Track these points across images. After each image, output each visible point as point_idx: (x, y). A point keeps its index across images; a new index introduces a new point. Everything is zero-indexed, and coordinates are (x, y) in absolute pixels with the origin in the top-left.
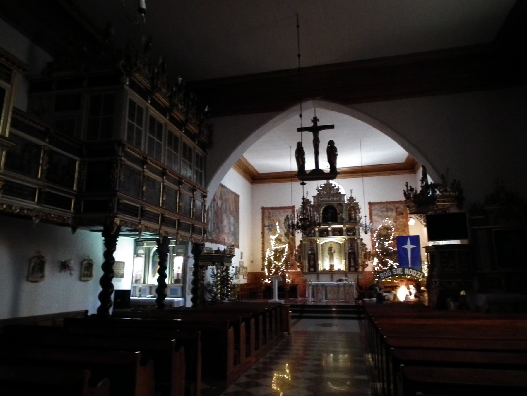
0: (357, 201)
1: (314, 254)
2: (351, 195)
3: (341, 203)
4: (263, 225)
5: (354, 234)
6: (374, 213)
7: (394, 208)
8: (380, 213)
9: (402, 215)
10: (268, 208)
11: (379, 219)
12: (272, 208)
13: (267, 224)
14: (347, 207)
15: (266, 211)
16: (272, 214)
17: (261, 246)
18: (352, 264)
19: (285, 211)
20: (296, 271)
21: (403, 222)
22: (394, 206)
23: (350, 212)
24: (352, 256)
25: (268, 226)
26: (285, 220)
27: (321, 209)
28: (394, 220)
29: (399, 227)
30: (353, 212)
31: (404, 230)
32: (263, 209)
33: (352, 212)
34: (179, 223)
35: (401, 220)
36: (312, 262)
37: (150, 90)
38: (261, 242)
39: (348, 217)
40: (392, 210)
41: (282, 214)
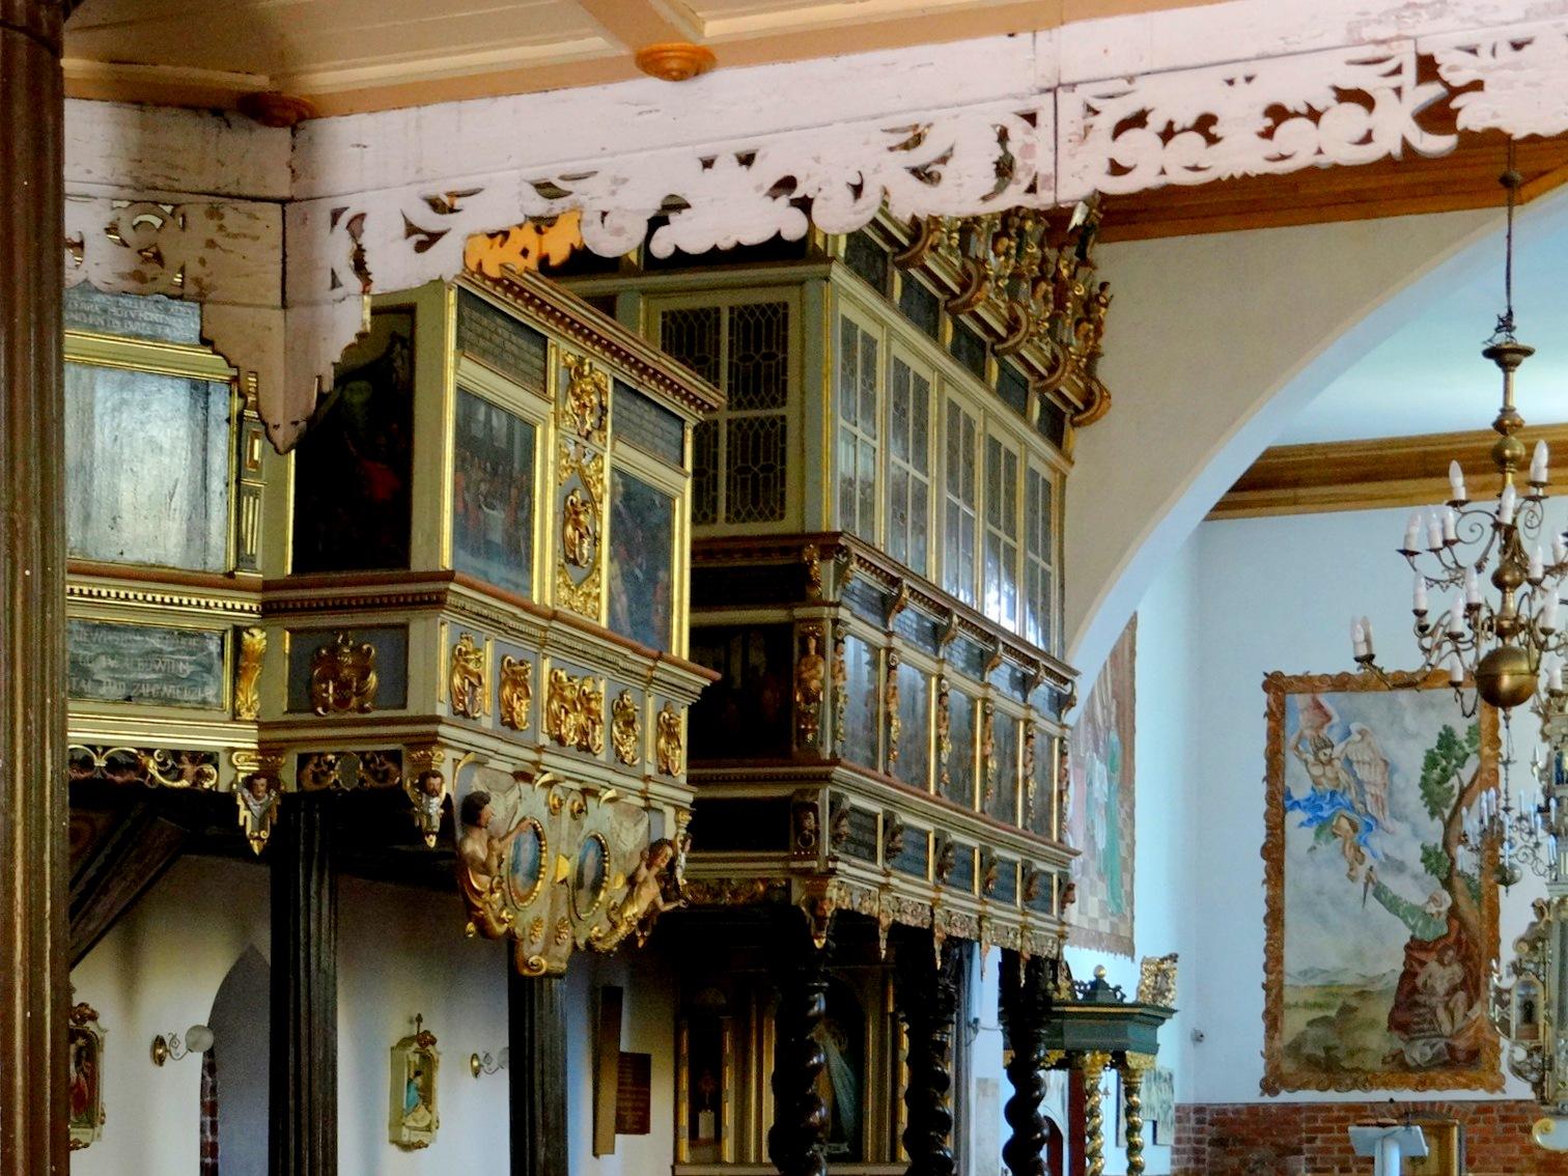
4: (1271, 798)
10: (1307, 683)
13: (1301, 790)
15: (1298, 702)
16: (1336, 719)
17: (1260, 932)
19: (1433, 706)
20: (1498, 1096)
25: (1313, 804)
26: (1431, 761)
32: (1276, 685)
34: (988, 863)
37: (905, 241)
38: (1263, 910)
41: (1410, 721)
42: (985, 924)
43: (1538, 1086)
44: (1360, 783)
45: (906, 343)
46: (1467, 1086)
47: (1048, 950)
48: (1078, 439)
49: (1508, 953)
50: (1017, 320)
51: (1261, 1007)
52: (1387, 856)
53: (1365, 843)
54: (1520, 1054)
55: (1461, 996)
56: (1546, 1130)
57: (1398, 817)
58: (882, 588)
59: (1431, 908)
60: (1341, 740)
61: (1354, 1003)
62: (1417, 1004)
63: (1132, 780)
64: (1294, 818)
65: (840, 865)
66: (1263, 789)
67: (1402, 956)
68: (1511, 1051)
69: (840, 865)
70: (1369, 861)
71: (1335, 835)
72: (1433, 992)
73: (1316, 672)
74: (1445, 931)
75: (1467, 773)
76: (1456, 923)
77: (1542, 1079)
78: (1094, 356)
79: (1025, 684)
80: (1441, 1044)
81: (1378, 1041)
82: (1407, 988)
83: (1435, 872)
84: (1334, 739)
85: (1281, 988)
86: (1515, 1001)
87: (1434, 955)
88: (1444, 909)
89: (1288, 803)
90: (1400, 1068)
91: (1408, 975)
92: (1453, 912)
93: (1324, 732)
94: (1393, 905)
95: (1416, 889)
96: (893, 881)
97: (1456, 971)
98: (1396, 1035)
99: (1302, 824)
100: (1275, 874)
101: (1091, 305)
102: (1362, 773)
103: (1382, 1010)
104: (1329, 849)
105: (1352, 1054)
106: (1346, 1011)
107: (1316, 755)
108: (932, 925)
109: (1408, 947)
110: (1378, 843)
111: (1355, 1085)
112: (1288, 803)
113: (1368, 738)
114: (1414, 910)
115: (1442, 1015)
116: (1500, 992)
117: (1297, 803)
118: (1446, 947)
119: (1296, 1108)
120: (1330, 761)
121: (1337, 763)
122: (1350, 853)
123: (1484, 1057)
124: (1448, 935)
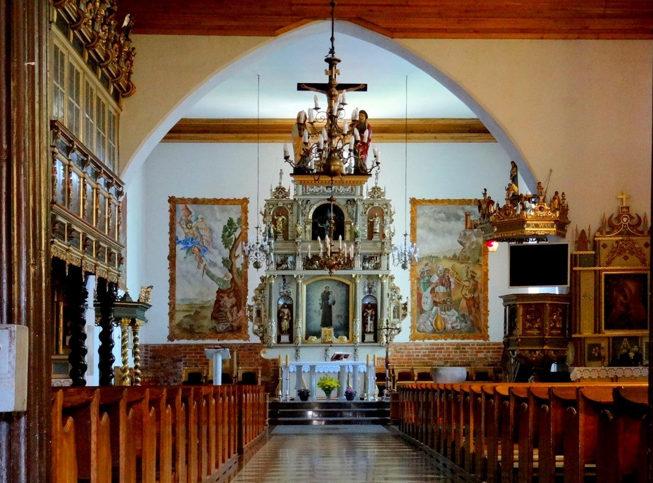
0: (387, 197)
1: (290, 307)
2: (376, 183)
3: (354, 200)
4: (171, 239)
5: (377, 267)
6: (420, 221)
7: (462, 213)
8: (432, 223)
9: (476, 230)
10: (183, 201)
11: (431, 236)
12: (195, 201)
13: (181, 236)
14: (367, 209)
15: (180, 207)
16: (193, 214)
17: (168, 285)
18: (370, 328)
20: (247, 342)
21: (477, 243)
22: (463, 208)
23: (372, 220)
24: (370, 312)
25: (185, 242)
26: (225, 230)
27: (310, 210)
28: (459, 240)
29: (468, 254)
30: (377, 220)
31: (478, 261)
32: (172, 200)
33: (377, 220)
35: (474, 239)
36: (285, 324)
38: (169, 278)
39: (366, 230)
40: (458, 218)
41: (218, 215)
42: (97, 268)
43: (262, 338)
44: (201, 236)
45: (74, 58)
46: (237, 339)
47: (115, 280)
48: (124, 102)
49: (251, 294)
50: (108, 55)
51: (168, 311)
52: (211, 261)
53: (203, 256)
54: (256, 327)
55: (235, 308)
56: (264, 353)
57: (215, 248)
58: (67, 143)
59: (226, 279)
60: (195, 221)
61: (200, 310)
62: (221, 311)
63: (126, 230)
64: (179, 247)
65: (55, 240)
66: (168, 236)
67: (215, 294)
68: (251, 326)
69: (55, 240)
70: (205, 262)
71: (193, 253)
72: (226, 308)
73: (186, 197)
74: (230, 287)
75: (237, 234)
76: (233, 284)
77: (263, 336)
78: (130, 73)
79: (108, 185)
80: (229, 324)
81: (207, 323)
82: (217, 306)
83: (227, 267)
84: (193, 220)
85: (174, 305)
86: (255, 310)
87: (226, 294)
88: (230, 279)
89: (177, 242)
90: (215, 333)
91: (217, 301)
92: (233, 280)
93: (189, 218)
94: (212, 277)
95: (220, 272)
96: (71, 248)
97: (234, 300)
98: (214, 321)
99: (182, 249)
100: (173, 266)
101: (129, 55)
102: (202, 232)
103: (208, 313)
104: (191, 258)
105: (199, 327)
106: (197, 313)
107: (186, 225)
108: (81, 266)
109: (217, 292)
110: (208, 257)
111: (199, 338)
112: (177, 242)
113: (204, 220)
114: (219, 279)
115: (229, 315)
116: (250, 306)
117: (180, 242)
118: (230, 292)
119: (180, 346)
120: (191, 228)
121: (194, 228)
122: (198, 259)
123: (243, 329)
124: (230, 288)
